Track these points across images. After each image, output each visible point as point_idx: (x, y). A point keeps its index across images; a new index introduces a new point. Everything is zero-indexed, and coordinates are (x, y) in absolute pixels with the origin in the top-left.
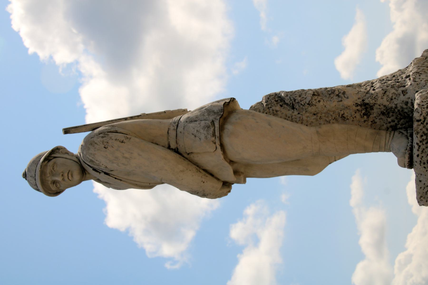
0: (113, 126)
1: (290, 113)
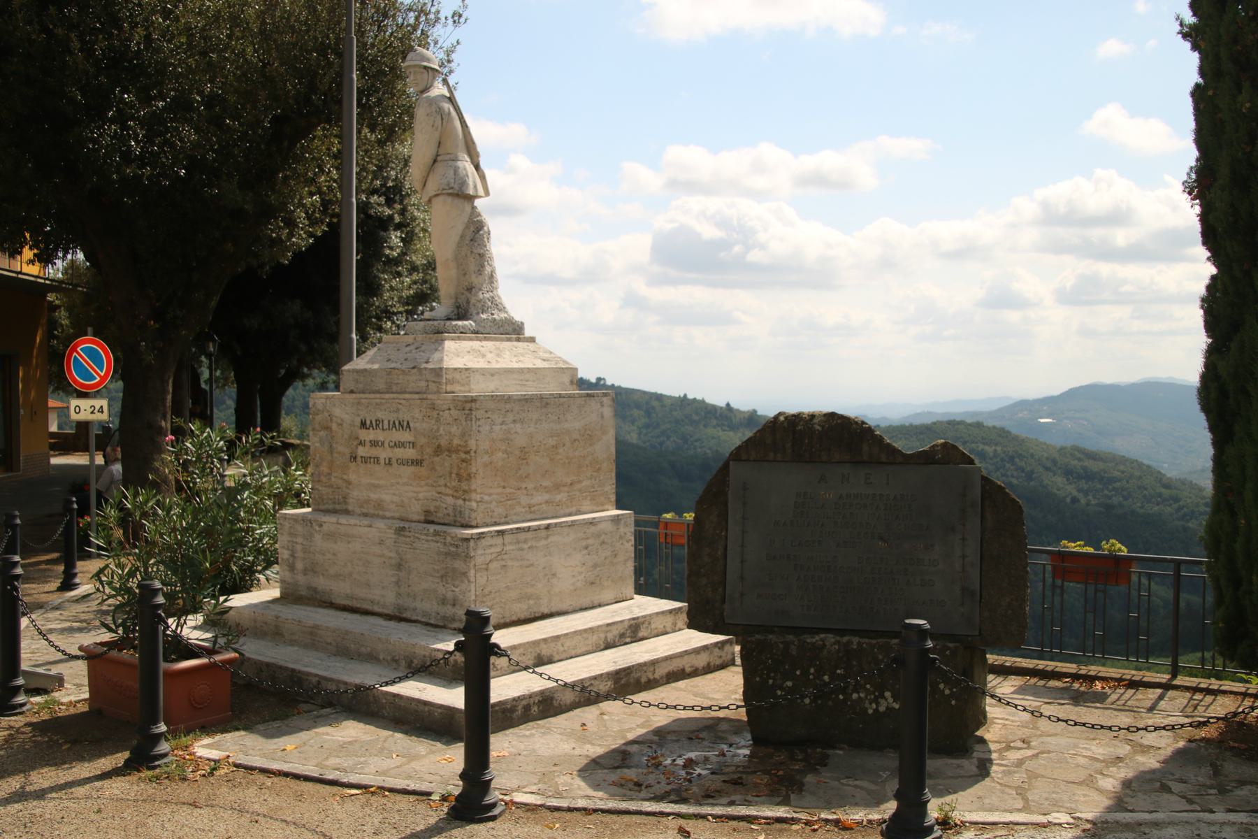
0: (449, 113)
1: (468, 238)
